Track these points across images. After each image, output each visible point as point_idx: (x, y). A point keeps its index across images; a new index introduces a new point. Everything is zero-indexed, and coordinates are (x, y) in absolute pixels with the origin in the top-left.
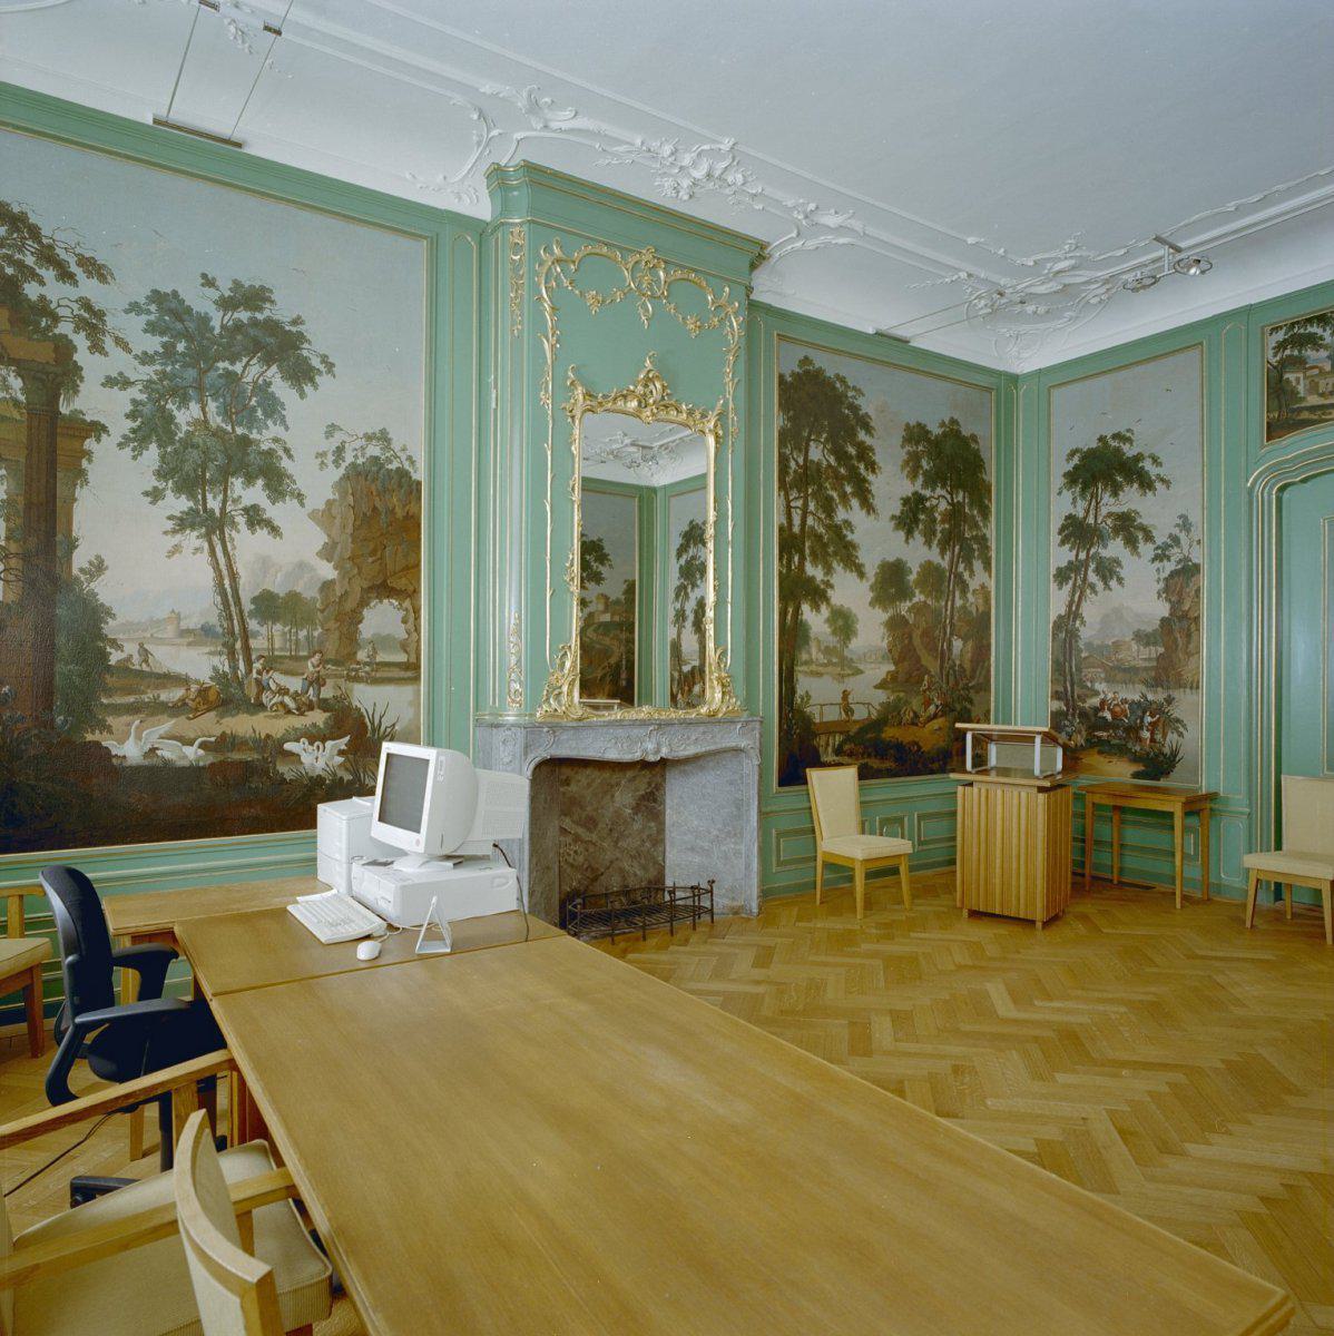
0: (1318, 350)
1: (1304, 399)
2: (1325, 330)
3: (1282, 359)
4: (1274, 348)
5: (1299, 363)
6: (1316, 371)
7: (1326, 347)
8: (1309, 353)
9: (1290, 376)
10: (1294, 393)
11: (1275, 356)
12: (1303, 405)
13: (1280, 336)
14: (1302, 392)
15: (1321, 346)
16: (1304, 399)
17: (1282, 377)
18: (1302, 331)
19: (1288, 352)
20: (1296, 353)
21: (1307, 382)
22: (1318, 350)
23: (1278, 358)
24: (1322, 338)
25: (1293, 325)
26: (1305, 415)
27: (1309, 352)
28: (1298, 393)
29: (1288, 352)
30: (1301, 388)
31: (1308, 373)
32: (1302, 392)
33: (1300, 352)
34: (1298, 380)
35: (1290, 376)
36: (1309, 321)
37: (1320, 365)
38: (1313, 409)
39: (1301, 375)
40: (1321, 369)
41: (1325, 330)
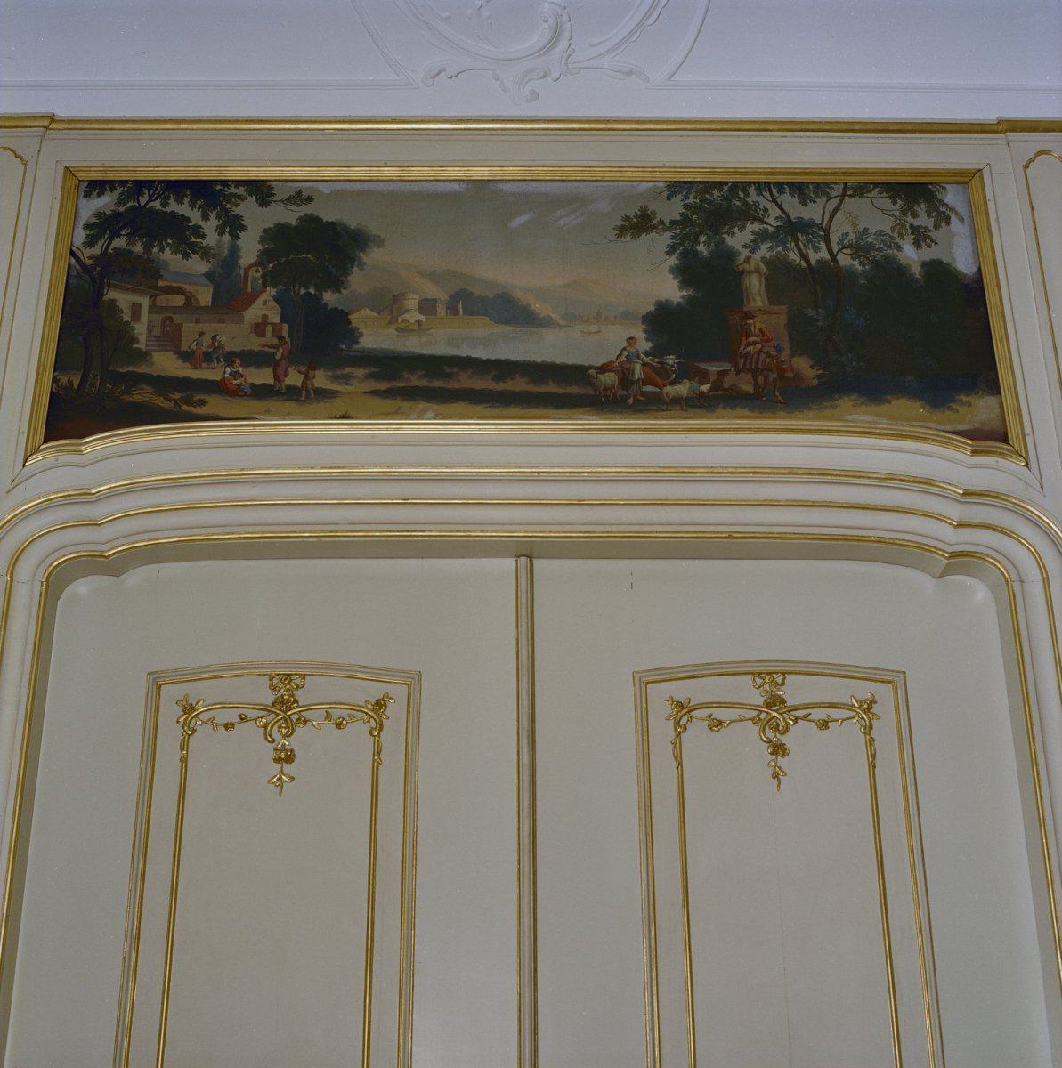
0: (186, 256)
1: (143, 356)
2: (205, 217)
3: (104, 253)
4: (88, 226)
5: (144, 274)
6: (179, 300)
7: (206, 253)
8: (168, 256)
9: (122, 298)
10: (124, 338)
11: (90, 242)
12: (143, 369)
13: (105, 202)
14: (143, 338)
15: (195, 248)
16: (143, 356)
17: (100, 294)
18: (157, 205)
19: (120, 242)
20: (138, 248)
21: (158, 318)
22: (186, 256)
23: (96, 250)
24: (197, 231)
25: (139, 186)
26: (143, 395)
27: (167, 254)
28: (134, 340)
29: (120, 242)
30: (140, 329)
31: (163, 300)
32: (143, 338)
33: (148, 247)
34: (136, 309)
35: (122, 298)
36: (176, 187)
37: (187, 287)
38: (165, 384)
39: (145, 301)
40: (190, 299)
41: (205, 217)
